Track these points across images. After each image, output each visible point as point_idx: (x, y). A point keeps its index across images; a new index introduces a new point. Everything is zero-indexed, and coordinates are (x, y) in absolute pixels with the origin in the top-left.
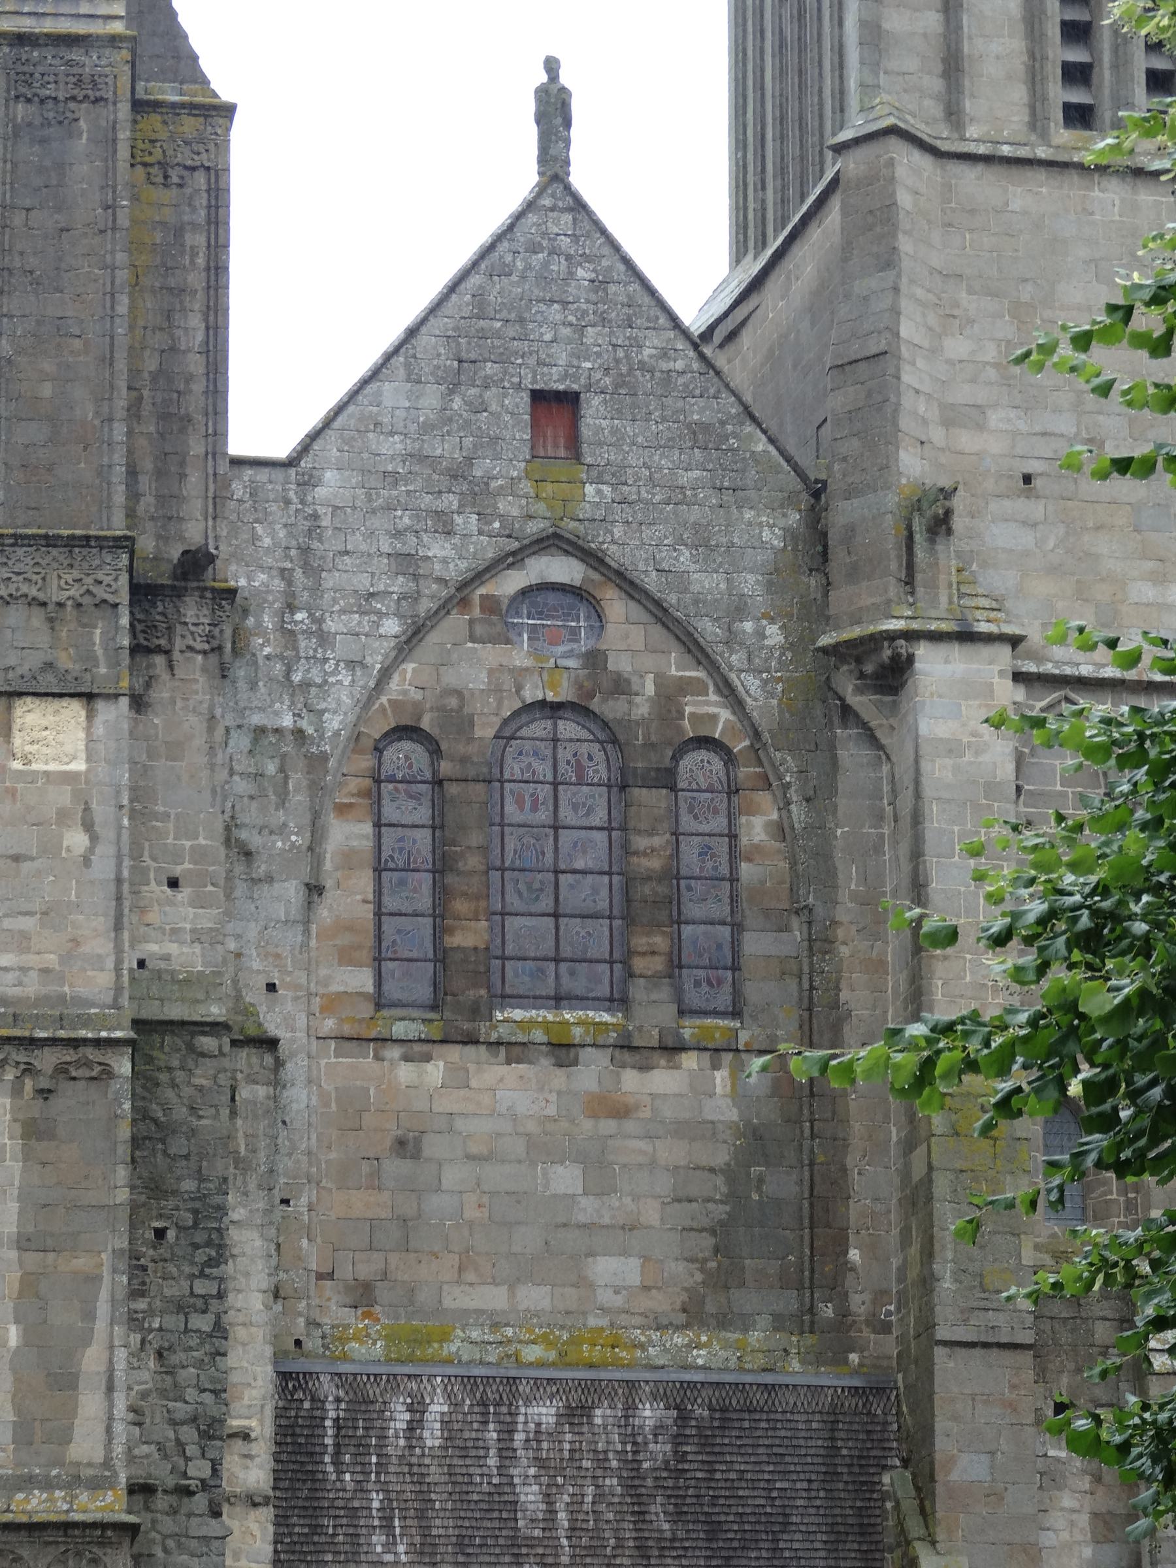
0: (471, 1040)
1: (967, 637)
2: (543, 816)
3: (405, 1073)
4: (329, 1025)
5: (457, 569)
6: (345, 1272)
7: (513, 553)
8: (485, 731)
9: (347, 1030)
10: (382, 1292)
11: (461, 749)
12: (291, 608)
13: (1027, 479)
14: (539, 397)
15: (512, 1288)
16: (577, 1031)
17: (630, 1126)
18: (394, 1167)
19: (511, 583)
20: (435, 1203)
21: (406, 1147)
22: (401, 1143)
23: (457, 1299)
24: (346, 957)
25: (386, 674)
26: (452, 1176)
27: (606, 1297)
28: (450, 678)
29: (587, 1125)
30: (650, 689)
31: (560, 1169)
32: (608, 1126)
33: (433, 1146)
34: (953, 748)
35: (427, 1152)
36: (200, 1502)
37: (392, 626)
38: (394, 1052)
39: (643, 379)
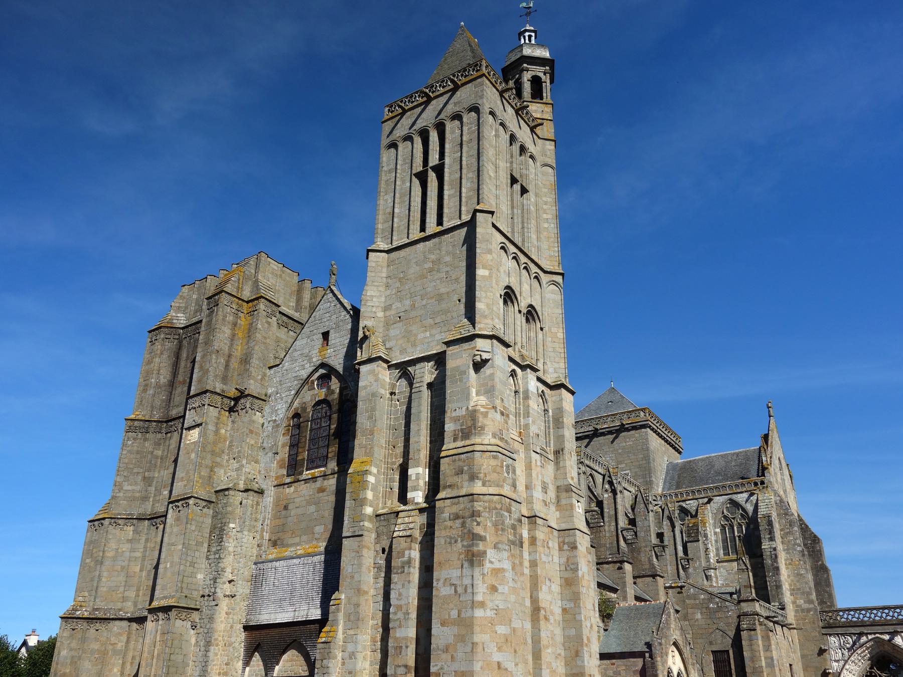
0: (299, 481)
1: (370, 360)
2: (319, 426)
3: (288, 490)
4: (275, 483)
5: (305, 376)
6: (273, 539)
7: (316, 369)
8: (309, 409)
9: (279, 484)
10: (279, 543)
11: (304, 415)
12: (277, 394)
13: (400, 317)
14: (323, 334)
15: (300, 536)
16: (317, 475)
17: (325, 494)
18: (284, 512)
19: (317, 375)
20: (290, 519)
21: (286, 508)
22: (285, 507)
23: (291, 541)
24: (281, 467)
25: (292, 402)
26: (293, 513)
27: (317, 536)
28: (304, 400)
29: (317, 495)
30: (338, 391)
31: (311, 507)
32: (321, 494)
33: (290, 507)
34: (365, 387)
35: (289, 508)
36: (211, 598)
37: (293, 392)
38: (286, 486)
39: (341, 323)
